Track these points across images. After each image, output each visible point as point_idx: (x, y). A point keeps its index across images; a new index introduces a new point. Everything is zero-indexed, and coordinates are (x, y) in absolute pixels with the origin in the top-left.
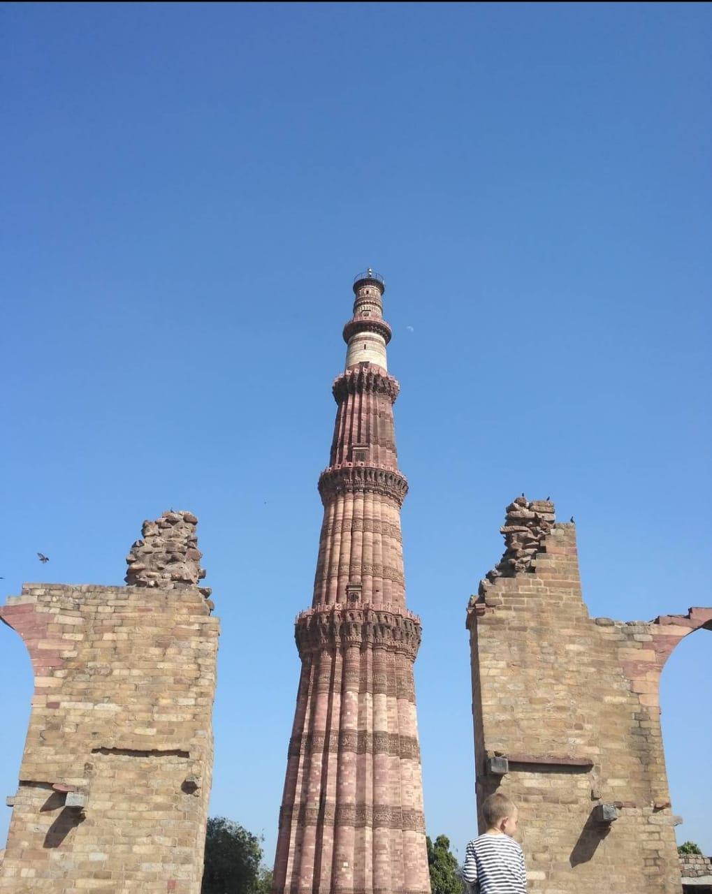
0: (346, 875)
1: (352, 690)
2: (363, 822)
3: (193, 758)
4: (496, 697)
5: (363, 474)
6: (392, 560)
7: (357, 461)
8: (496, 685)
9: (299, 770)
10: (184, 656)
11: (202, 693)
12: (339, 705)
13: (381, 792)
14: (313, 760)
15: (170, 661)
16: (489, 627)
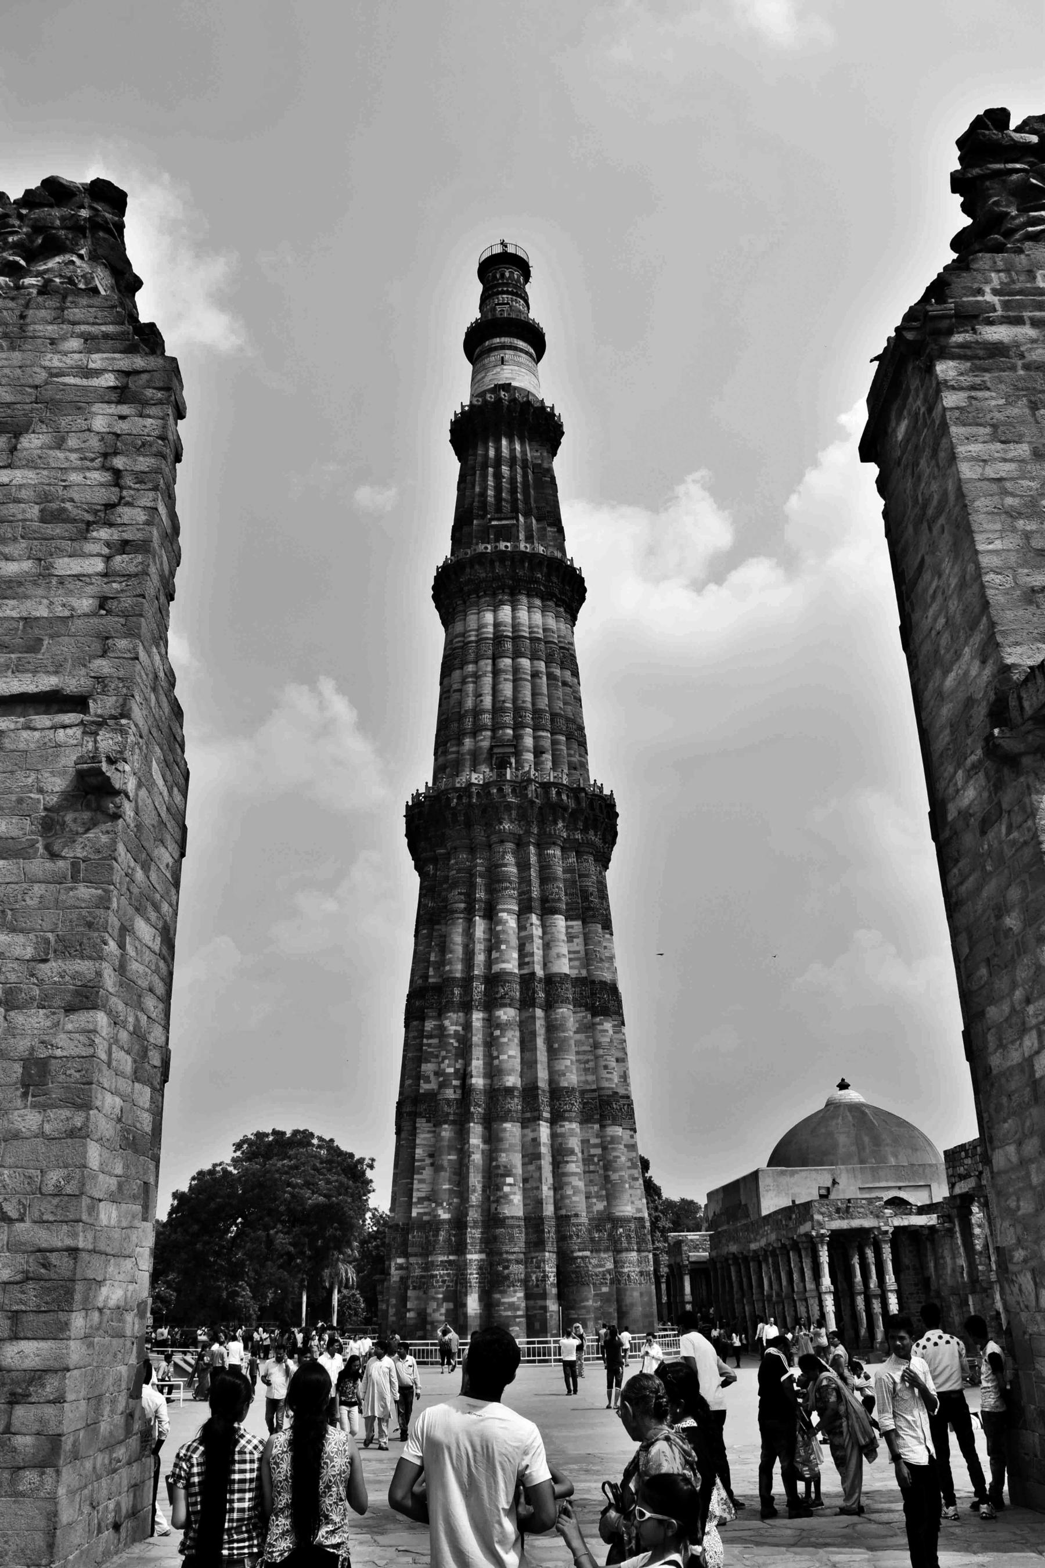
0: (512, 1197)
1: (509, 911)
2: (536, 1114)
3: (99, 711)
4: (1014, 530)
5: (508, 563)
6: (564, 704)
7: (497, 540)
8: (1009, 501)
9: (425, 1041)
10: (71, 451)
11: (125, 543)
12: (487, 937)
13: (563, 1068)
14: (447, 1023)
15: (31, 464)
16: (969, 364)
